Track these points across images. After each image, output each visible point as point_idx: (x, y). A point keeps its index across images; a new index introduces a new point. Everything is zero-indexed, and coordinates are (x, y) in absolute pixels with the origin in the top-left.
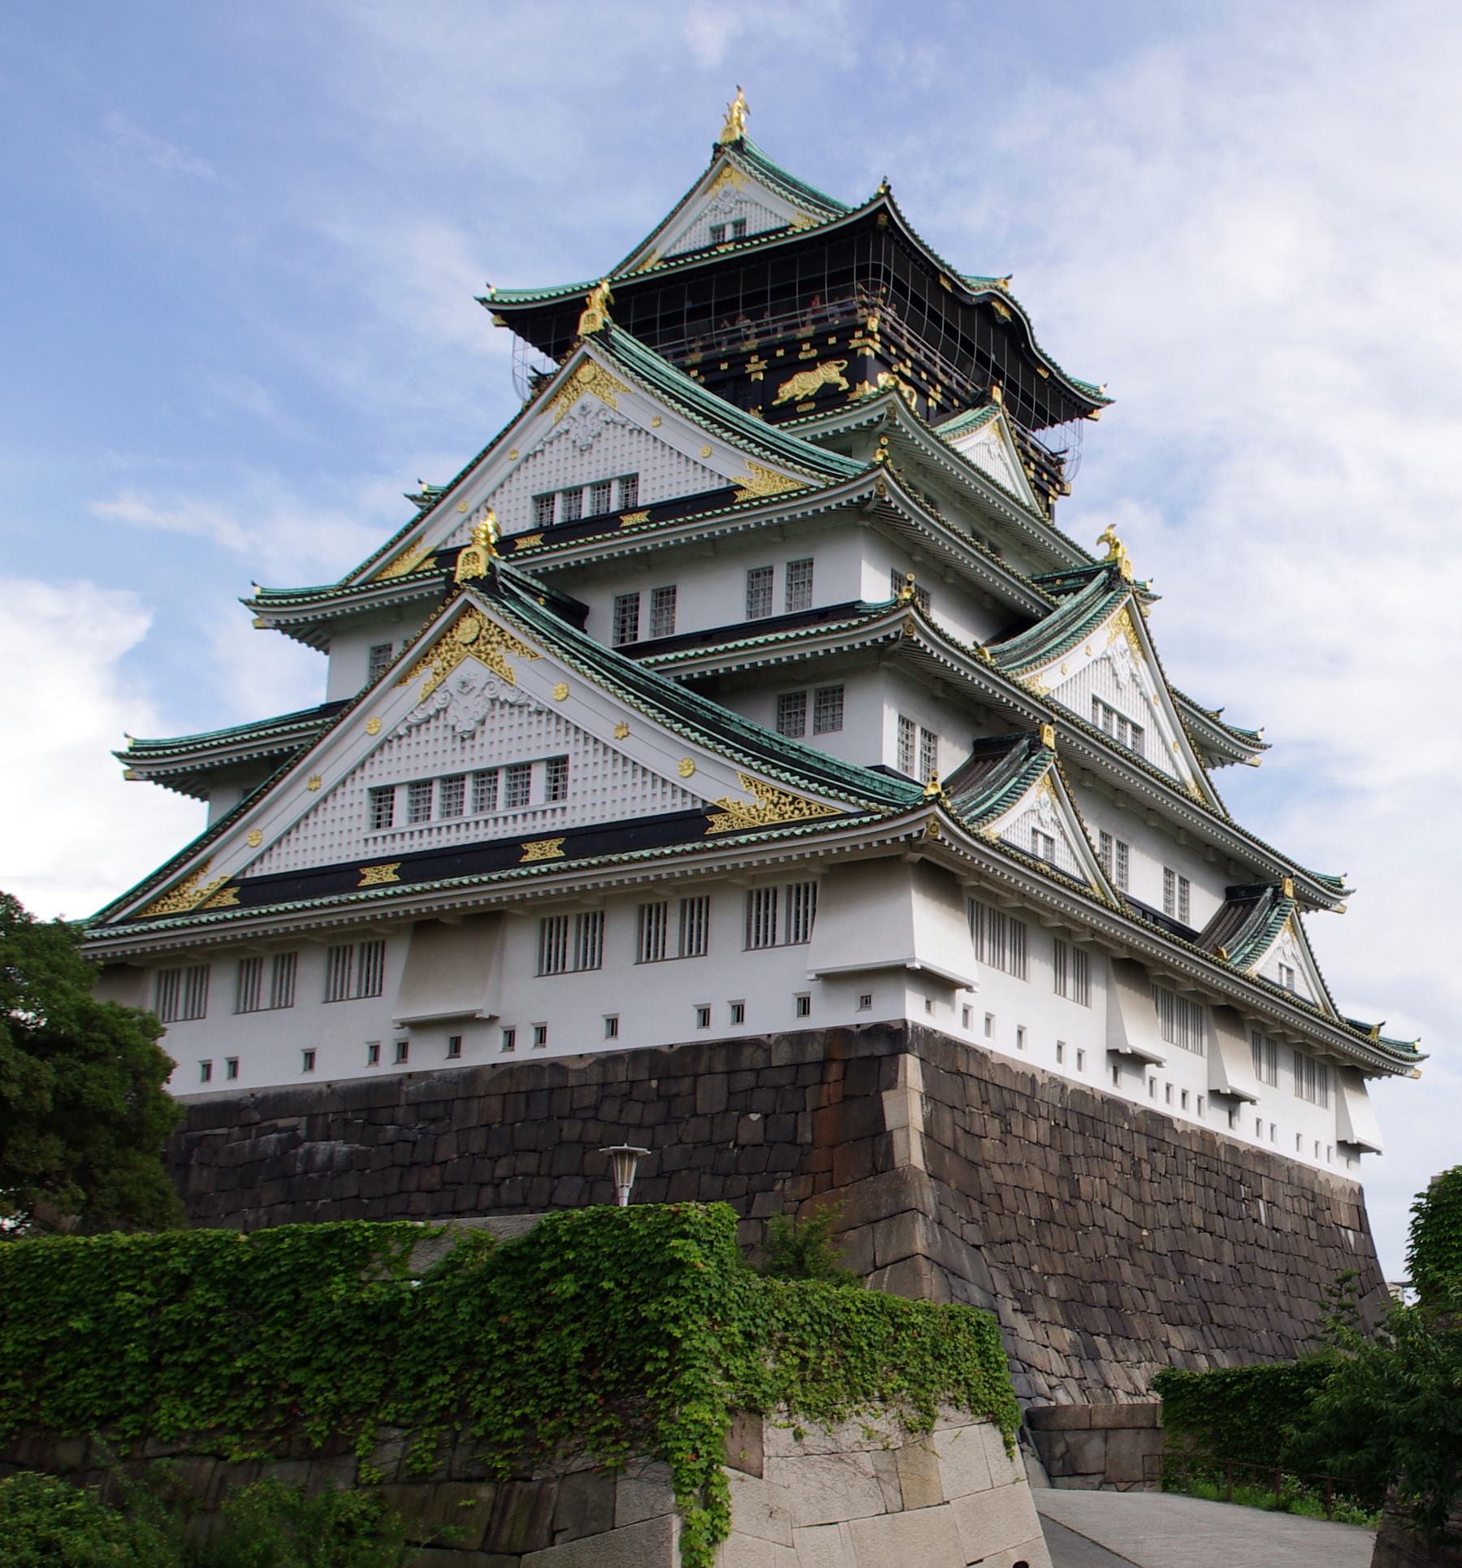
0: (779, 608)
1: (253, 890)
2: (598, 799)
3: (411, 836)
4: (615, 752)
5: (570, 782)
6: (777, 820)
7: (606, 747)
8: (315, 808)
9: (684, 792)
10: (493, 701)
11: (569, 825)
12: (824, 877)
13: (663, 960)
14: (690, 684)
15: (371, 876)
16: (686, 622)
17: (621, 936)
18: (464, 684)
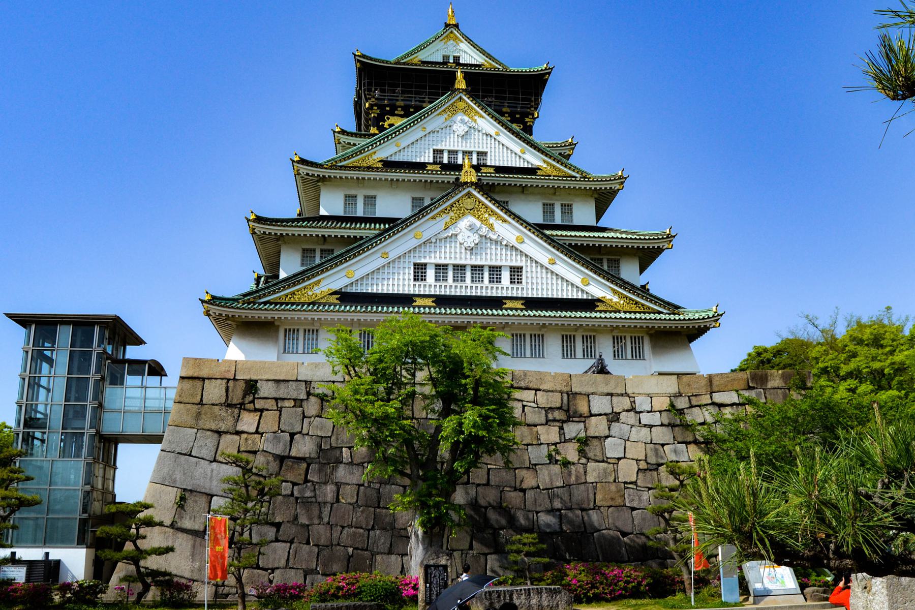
0: (558, 221)
1: (346, 297)
2: (537, 285)
3: (431, 285)
4: (547, 268)
5: (524, 277)
6: (628, 309)
7: (542, 266)
8: (384, 266)
9: (583, 291)
10: (481, 236)
11: (525, 296)
12: (651, 336)
13: (575, 358)
14: (570, 245)
15: (419, 302)
17: (553, 346)
18: (470, 226)
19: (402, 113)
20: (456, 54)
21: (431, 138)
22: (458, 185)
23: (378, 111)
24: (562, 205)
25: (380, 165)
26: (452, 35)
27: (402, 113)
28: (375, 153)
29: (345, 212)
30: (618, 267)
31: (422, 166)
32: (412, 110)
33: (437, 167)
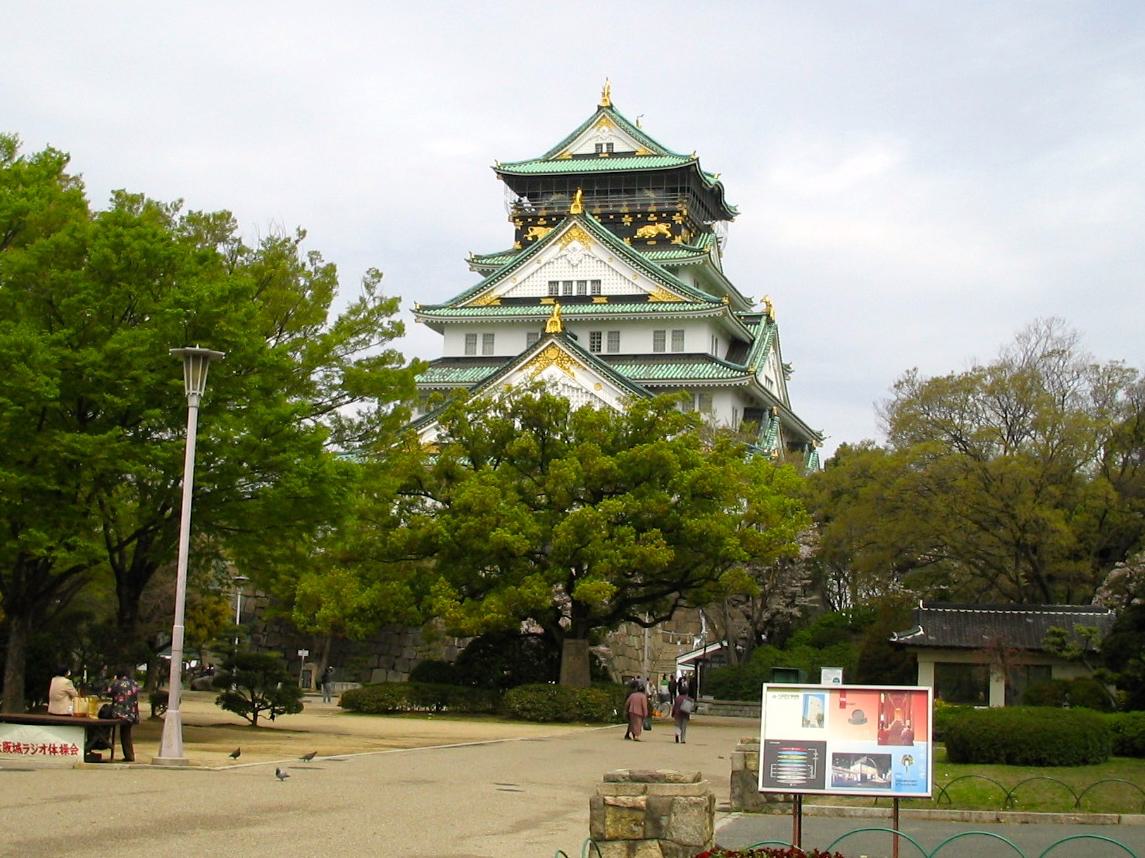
0: (668, 350)
14: (652, 389)
16: (626, 348)
19: (545, 222)
20: (610, 142)
21: (547, 270)
22: (546, 336)
23: (521, 223)
24: (674, 332)
25: (498, 303)
26: (604, 120)
27: (545, 222)
28: (492, 290)
29: (466, 352)
30: (711, 402)
31: (534, 301)
32: (554, 219)
33: (551, 301)
